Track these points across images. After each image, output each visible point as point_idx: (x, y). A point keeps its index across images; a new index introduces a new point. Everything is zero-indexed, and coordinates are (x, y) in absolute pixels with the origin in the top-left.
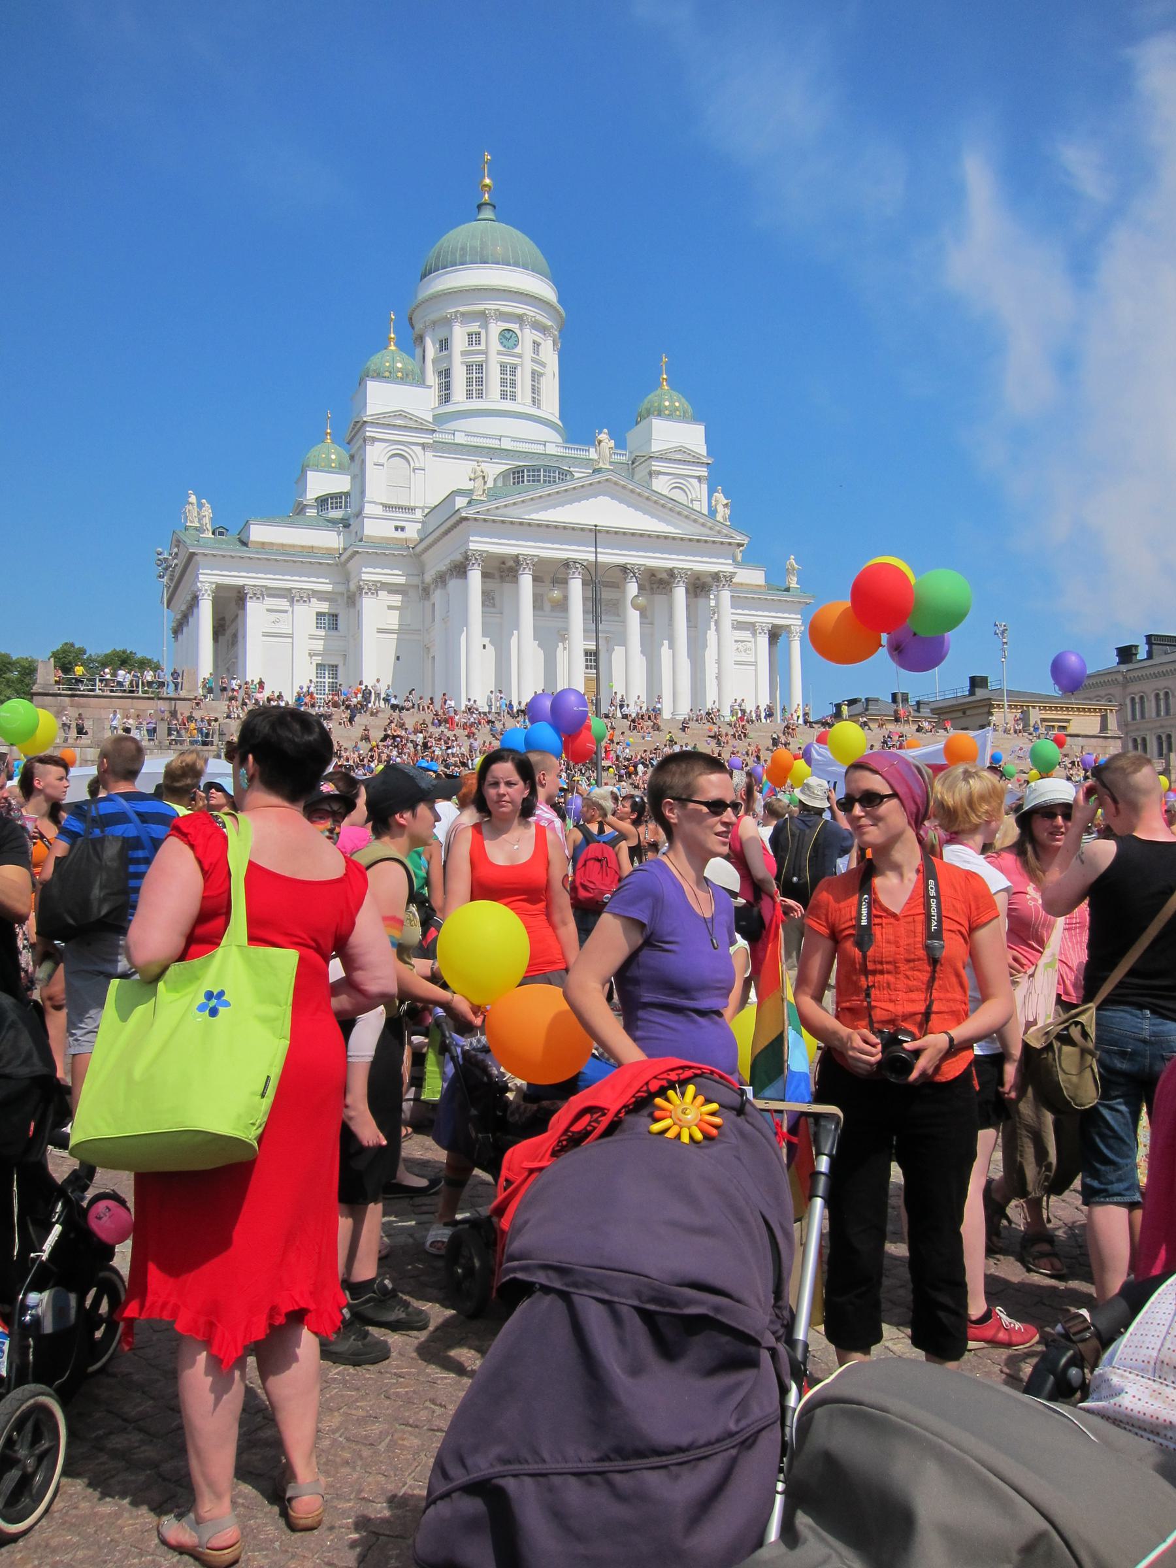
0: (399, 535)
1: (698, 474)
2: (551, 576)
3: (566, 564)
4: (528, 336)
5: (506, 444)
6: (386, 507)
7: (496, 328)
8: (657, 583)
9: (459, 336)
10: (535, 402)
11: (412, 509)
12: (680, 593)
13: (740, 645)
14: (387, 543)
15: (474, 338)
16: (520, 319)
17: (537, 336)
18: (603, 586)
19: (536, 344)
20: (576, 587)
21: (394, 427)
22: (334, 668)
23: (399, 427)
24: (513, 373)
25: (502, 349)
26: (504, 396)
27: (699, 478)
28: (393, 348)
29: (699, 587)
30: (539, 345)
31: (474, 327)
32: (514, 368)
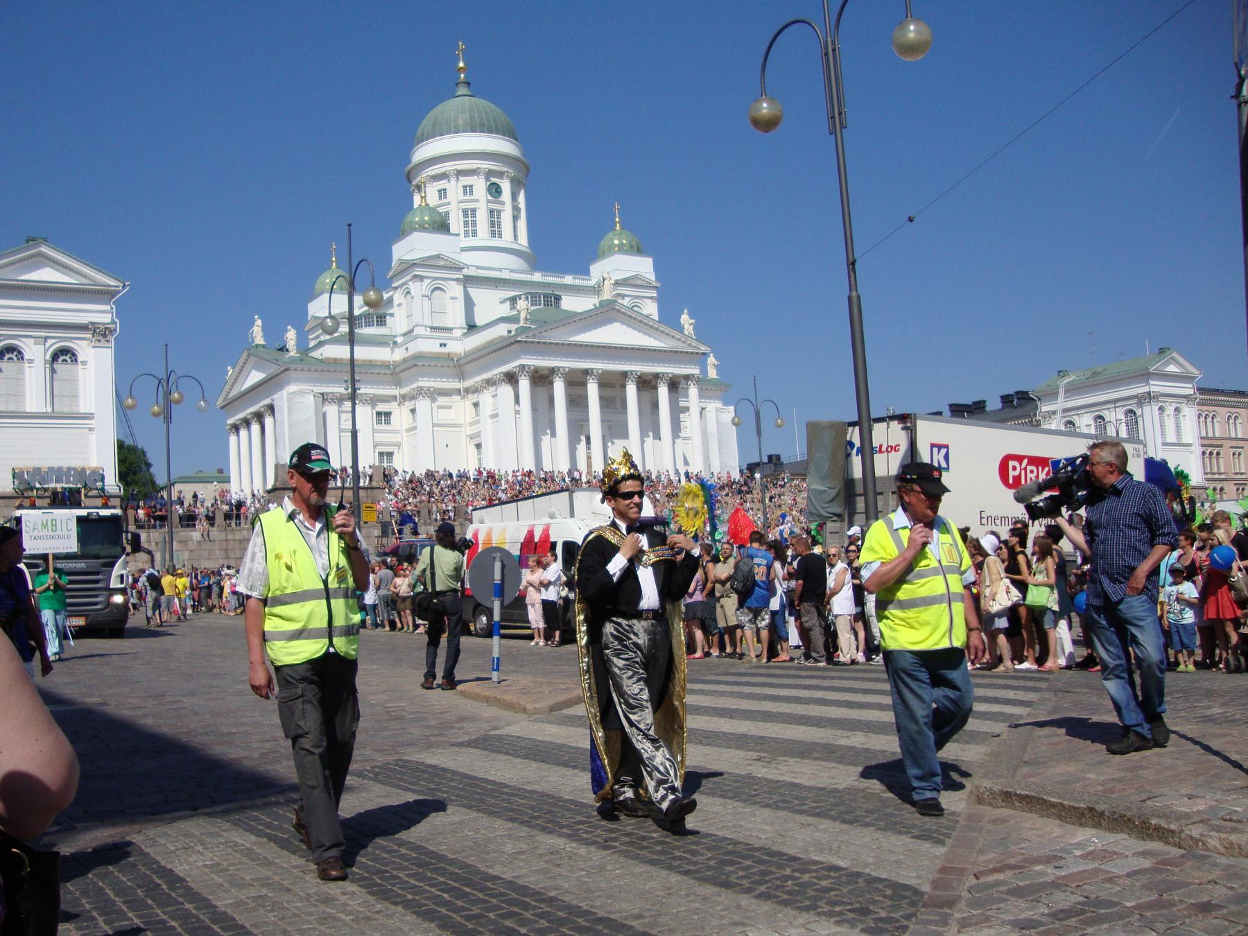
0: (443, 350)
3: (586, 372)
5: (505, 275)
6: (432, 328)
8: (647, 384)
10: (515, 236)
11: (450, 330)
12: (663, 391)
14: (436, 357)
15: (468, 189)
20: (593, 389)
22: (390, 454)
24: (499, 217)
26: (493, 235)
29: (675, 385)
32: (499, 212)
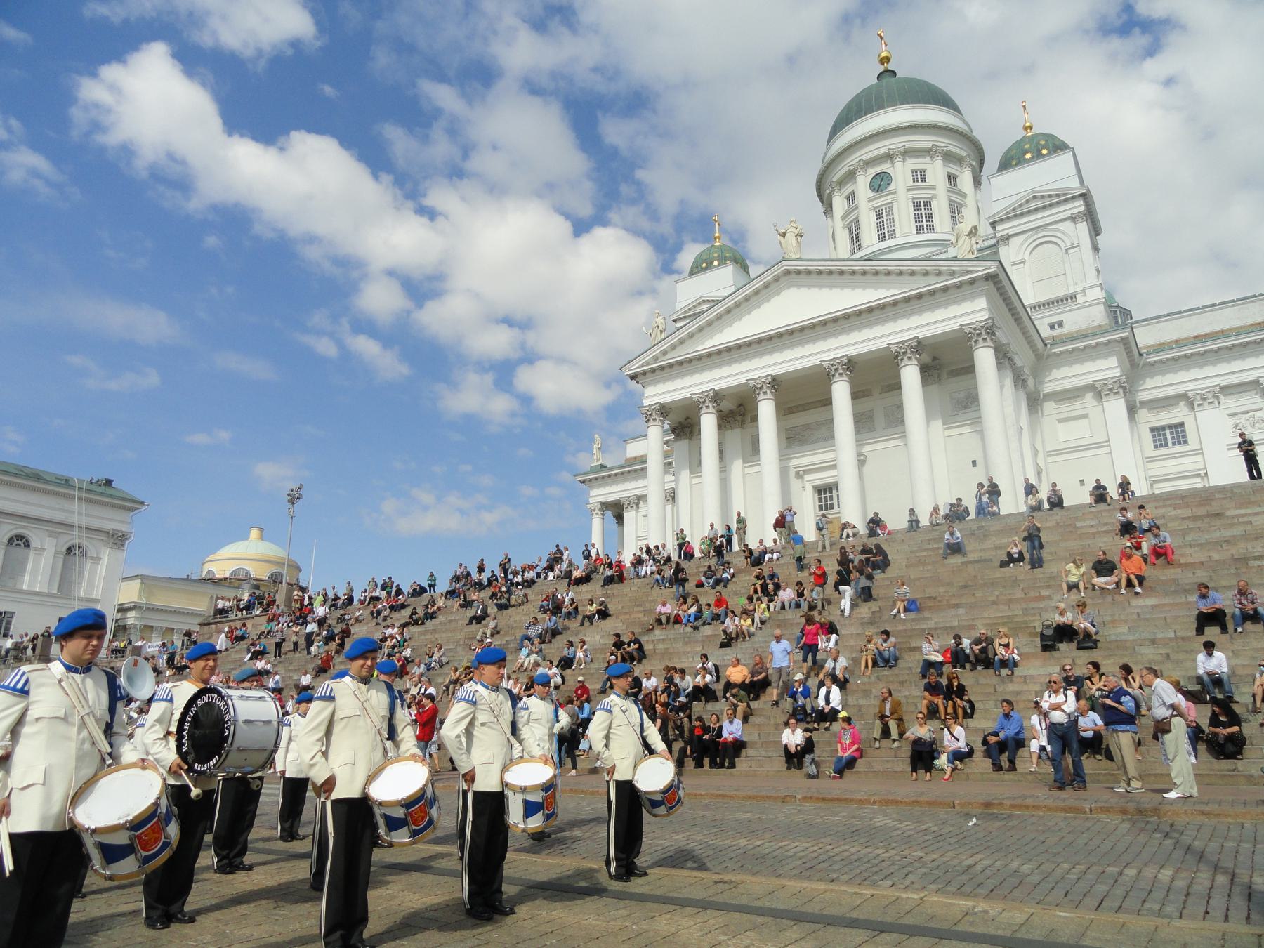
1: (1068, 214)
2: (736, 412)
4: (901, 173)
16: (889, 157)
26: (881, 238)
27: (1073, 219)
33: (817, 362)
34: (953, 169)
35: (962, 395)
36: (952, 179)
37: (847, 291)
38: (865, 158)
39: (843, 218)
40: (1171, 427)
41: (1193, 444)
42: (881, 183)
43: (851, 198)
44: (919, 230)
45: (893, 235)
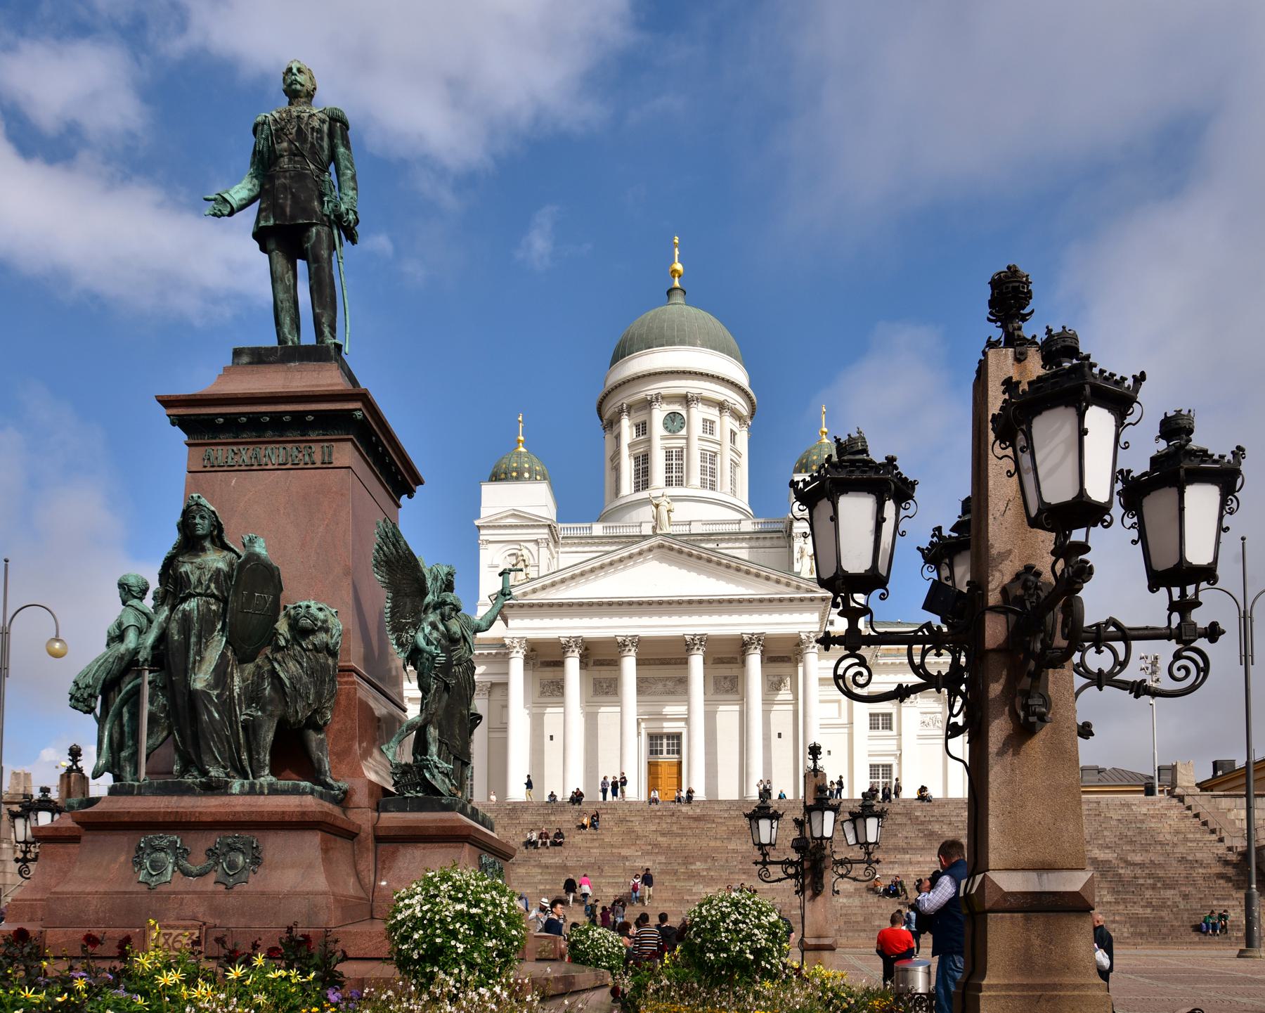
2: (600, 658)
7: (659, 414)
8: (727, 657)
9: (627, 429)
13: (927, 718)
16: (686, 400)
17: (713, 413)
18: (664, 661)
19: (709, 425)
21: (505, 527)
23: (511, 527)
24: (680, 457)
25: (666, 433)
26: (669, 482)
28: (522, 449)
30: (712, 422)
31: (640, 417)
33: (680, 634)
34: (735, 425)
35: (776, 679)
36: (733, 434)
37: (712, 580)
38: (663, 392)
39: (630, 446)
40: (883, 715)
41: (894, 732)
42: (674, 422)
43: (643, 428)
44: (703, 486)
45: (680, 483)
